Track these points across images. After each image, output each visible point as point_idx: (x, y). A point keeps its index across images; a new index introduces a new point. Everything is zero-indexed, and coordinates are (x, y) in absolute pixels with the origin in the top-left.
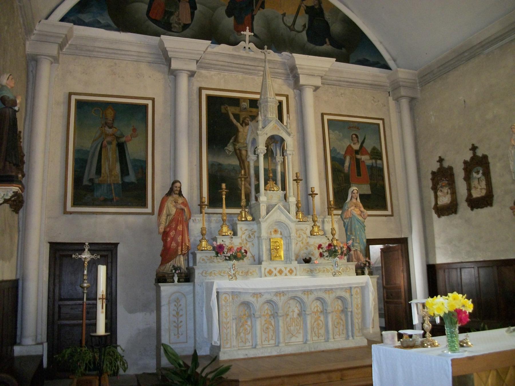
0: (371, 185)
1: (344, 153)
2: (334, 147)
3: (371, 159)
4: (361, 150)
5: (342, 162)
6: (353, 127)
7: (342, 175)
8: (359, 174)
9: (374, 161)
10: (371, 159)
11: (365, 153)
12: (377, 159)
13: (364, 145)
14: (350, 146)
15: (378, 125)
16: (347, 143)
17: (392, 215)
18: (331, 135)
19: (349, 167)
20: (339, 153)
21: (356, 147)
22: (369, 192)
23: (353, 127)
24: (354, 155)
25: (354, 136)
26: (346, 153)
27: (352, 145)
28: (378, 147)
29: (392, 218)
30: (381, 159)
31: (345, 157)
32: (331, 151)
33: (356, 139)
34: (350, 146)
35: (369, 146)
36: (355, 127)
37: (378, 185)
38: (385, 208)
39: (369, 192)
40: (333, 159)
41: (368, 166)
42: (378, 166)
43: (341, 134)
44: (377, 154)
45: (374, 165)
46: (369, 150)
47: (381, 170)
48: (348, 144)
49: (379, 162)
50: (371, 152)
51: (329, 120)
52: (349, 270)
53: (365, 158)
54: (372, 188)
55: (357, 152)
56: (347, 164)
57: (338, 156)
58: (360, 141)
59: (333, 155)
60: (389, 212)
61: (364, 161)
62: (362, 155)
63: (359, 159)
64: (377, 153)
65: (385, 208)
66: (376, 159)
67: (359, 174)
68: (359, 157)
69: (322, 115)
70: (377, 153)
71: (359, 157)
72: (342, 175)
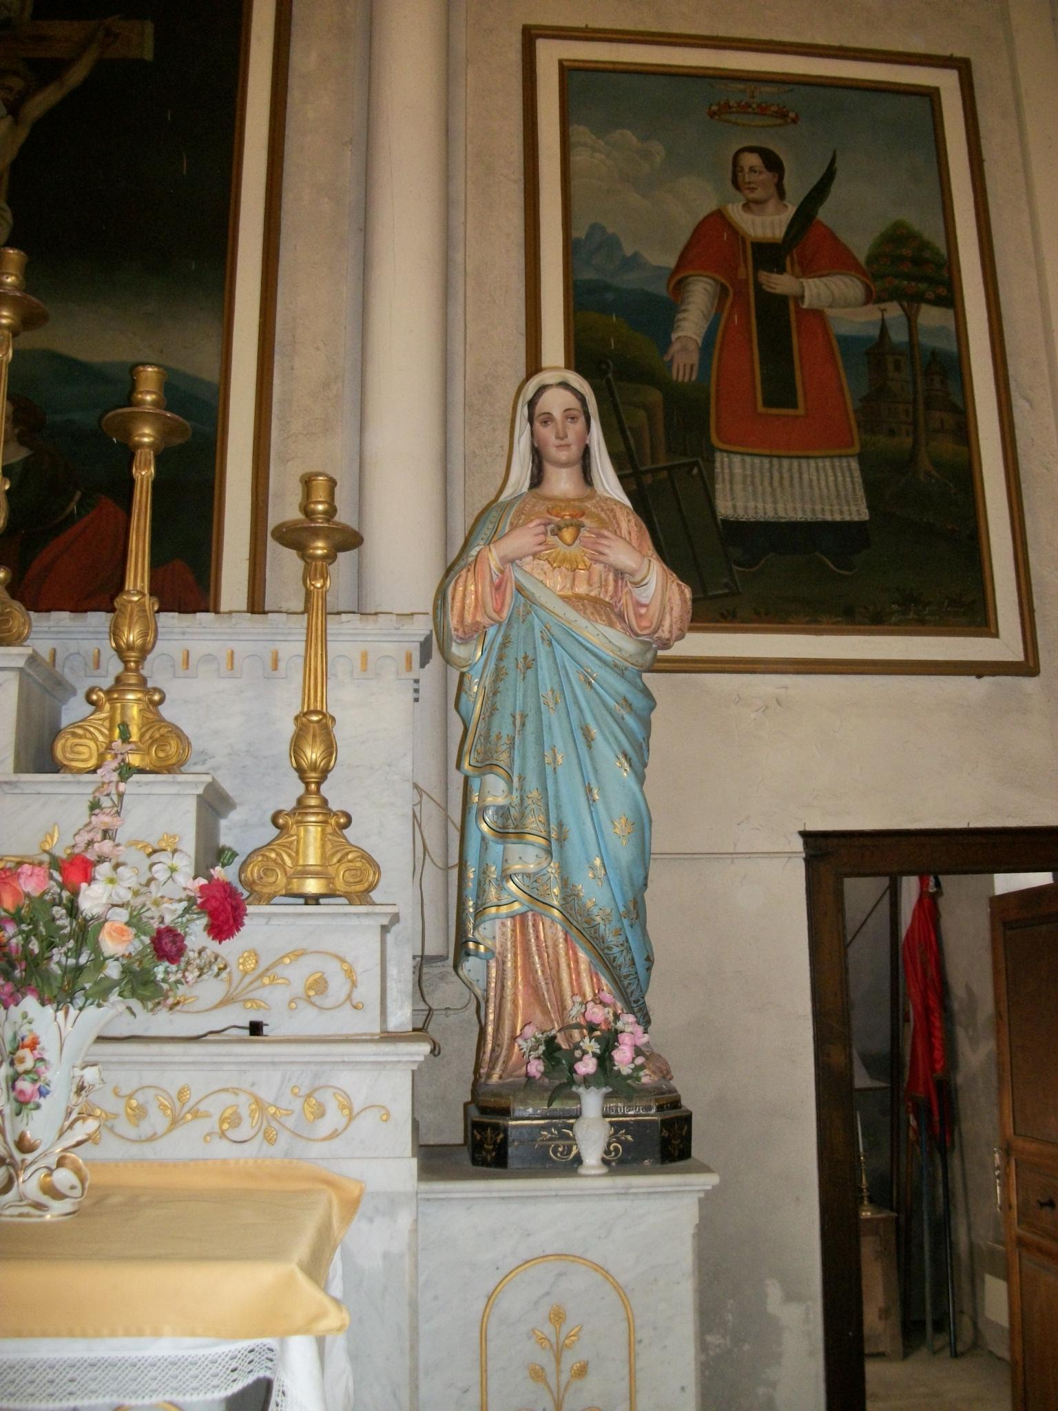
0: (862, 459)
1: (671, 261)
2: (594, 228)
3: (871, 298)
4: (805, 243)
5: (659, 315)
6: (744, 108)
7: (654, 396)
8: (780, 391)
9: (894, 311)
10: (871, 298)
11: (838, 259)
12: (920, 298)
13: (824, 214)
14: (719, 218)
15: (931, 96)
16: (694, 199)
17: (1028, 667)
18: (579, 158)
19: (706, 347)
20: (633, 262)
21: (769, 224)
22: (855, 510)
23: (744, 108)
24: (745, 271)
25: (752, 160)
26: (684, 260)
27: (736, 213)
28: (932, 232)
29: (1027, 684)
30: (951, 298)
31: (679, 287)
32: (570, 248)
33: (766, 176)
34: (719, 218)
35: (861, 212)
36: (762, 111)
37: (925, 463)
38: (975, 615)
39: (858, 511)
40: (580, 297)
41: (847, 342)
42: (924, 339)
43: (658, 149)
44: (916, 270)
45: (899, 336)
46: (861, 246)
47: (952, 368)
48: (707, 206)
49: (931, 317)
50: (872, 259)
51: (567, 71)
52: (333, 1118)
53: (834, 299)
54: (872, 489)
55: (769, 256)
56: (691, 325)
57: (630, 280)
58: (797, 186)
59: (588, 275)
60: (1006, 644)
61: (817, 314)
62: (808, 269)
63: (783, 300)
64: (917, 261)
65: (975, 615)
66: (911, 301)
67: (780, 391)
68: (782, 283)
69: (530, 36)
70: (917, 261)
71: (782, 283)
72: (654, 396)
